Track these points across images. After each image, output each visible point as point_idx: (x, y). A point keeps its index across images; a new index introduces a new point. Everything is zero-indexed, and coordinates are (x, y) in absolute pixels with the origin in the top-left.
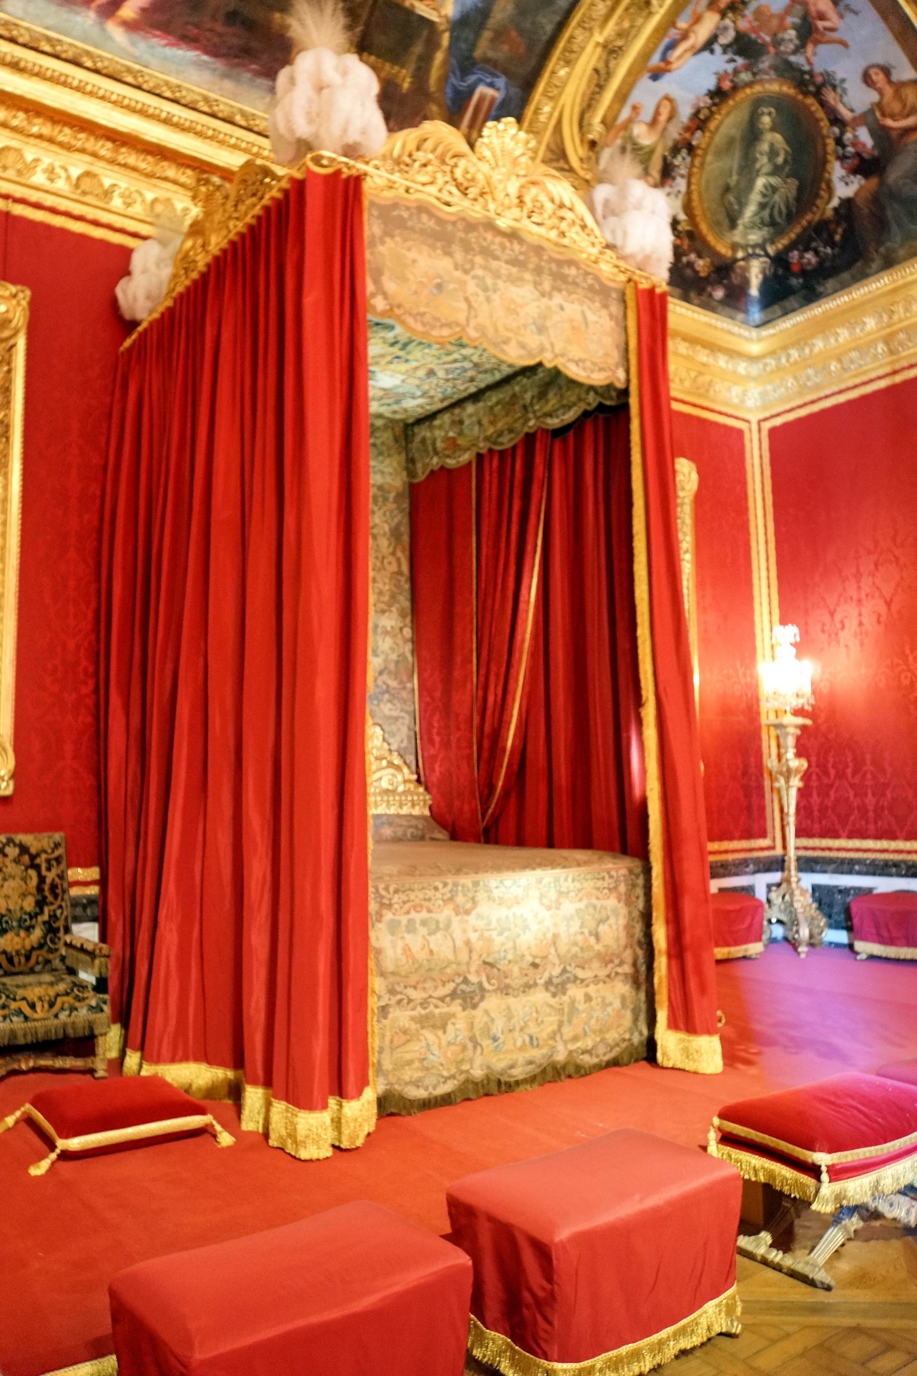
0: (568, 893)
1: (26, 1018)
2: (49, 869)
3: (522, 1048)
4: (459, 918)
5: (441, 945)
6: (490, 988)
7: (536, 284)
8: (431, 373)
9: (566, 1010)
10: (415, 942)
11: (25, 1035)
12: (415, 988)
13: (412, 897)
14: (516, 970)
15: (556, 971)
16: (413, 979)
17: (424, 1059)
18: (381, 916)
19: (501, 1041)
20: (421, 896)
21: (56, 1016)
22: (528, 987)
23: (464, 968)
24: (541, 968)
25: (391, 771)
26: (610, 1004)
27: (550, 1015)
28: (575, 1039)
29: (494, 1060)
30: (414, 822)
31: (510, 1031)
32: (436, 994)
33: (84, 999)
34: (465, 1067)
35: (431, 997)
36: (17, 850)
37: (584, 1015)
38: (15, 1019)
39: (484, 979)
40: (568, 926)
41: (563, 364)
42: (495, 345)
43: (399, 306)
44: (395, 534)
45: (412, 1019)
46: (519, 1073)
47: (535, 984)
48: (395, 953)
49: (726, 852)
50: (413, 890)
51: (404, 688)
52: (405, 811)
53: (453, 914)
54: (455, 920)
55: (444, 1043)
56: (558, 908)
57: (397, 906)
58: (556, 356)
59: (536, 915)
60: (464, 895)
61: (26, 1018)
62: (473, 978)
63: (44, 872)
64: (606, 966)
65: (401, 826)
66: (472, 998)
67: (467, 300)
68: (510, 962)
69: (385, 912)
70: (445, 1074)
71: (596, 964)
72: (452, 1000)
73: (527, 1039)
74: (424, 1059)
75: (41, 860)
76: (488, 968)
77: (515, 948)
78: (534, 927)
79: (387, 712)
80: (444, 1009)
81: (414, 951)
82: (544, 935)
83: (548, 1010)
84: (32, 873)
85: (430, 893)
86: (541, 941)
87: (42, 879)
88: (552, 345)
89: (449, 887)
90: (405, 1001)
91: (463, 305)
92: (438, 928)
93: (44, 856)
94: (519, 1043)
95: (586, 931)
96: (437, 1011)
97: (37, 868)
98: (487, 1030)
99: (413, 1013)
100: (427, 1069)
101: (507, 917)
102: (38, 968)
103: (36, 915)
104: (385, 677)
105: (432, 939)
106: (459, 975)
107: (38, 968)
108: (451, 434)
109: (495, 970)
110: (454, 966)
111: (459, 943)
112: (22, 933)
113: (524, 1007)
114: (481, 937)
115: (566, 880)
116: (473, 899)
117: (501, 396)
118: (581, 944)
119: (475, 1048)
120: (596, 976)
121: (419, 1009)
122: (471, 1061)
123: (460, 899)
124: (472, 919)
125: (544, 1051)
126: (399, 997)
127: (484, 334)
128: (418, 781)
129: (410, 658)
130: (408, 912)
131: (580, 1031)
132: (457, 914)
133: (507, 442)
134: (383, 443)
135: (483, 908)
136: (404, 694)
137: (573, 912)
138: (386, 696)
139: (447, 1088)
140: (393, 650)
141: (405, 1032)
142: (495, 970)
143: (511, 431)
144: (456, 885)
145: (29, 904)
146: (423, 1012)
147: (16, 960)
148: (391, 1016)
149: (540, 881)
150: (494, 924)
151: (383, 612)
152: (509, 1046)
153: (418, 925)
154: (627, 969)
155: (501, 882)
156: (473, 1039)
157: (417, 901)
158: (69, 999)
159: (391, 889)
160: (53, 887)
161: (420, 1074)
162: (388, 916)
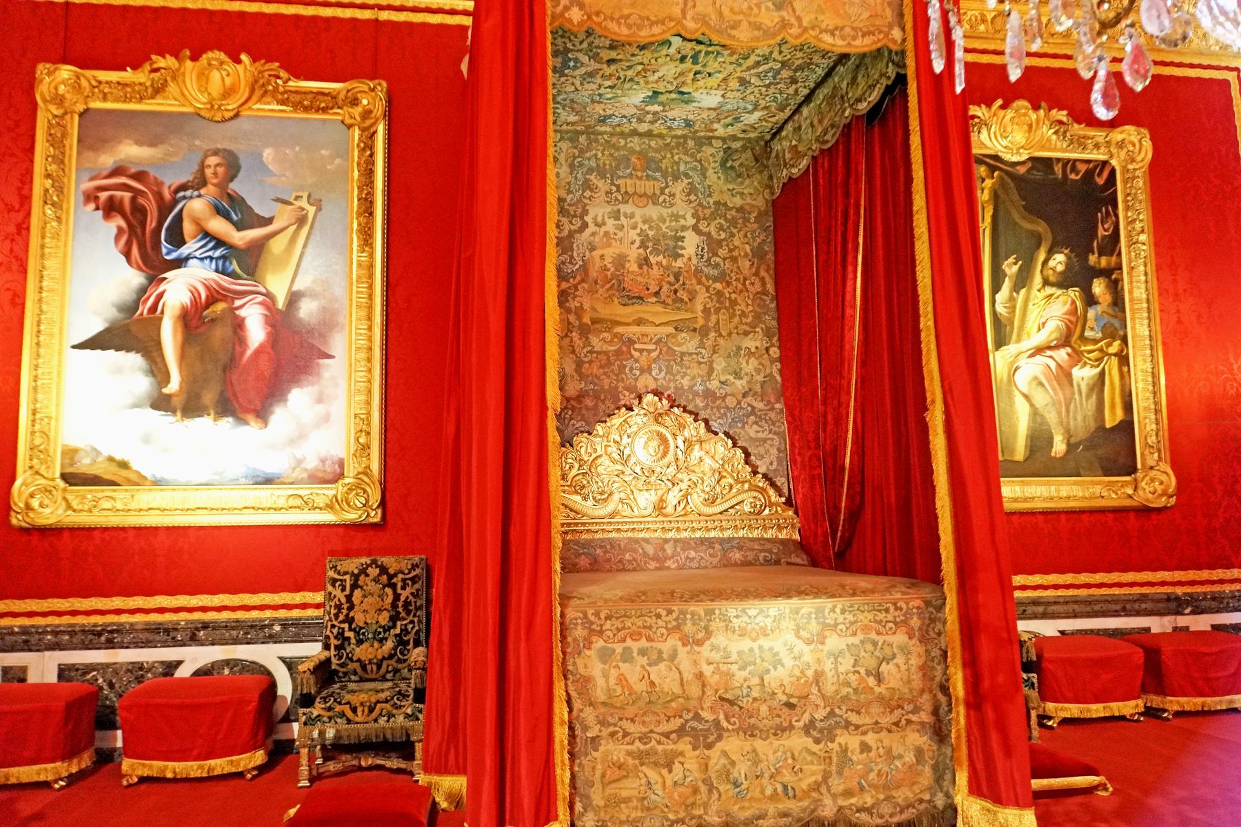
0: (836, 625)
1: (349, 721)
2: (403, 588)
3: (774, 797)
6: (730, 727)
8: (743, 82)
9: (835, 759)
11: (377, 737)
12: (633, 721)
13: (628, 624)
14: (764, 709)
15: (820, 714)
16: (631, 711)
17: (644, 799)
19: (743, 787)
20: (640, 624)
21: (376, 720)
22: (781, 730)
23: (694, 703)
24: (798, 710)
25: (755, 494)
26: (900, 757)
27: (812, 763)
28: (848, 793)
29: (736, 808)
30: (768, 546)
31: (757, 777)
32: (658, 730)
33: (401, 707)
34: (697, 812)
35: (652, 731)
36: (378, 570)
37: (860, 767)
38: (339, 720)
39: (722, 717)
40: (836, 662)
41: (816, 37)
42: (720, 32)
44: (758, 253)
45: (629, 753)
47: (791, 727)
48: (607, 682)
49: (1221, 582)
50: (629, 617)
51: (773, 409)
52: (770, 534)
53: (679, 643)
54: (682, 651)
55: (669, 783)
58: (805, 30)
59: (791, 650)
60: (694, 624)
61: (349, 721)
62: (706, 715)
63: (399, 591)
64: (891, 712)
65: (753, 550)
66: (706, 737)
68: (755, 699)
69: (594, 639)
70: (671, 816)
71: (876, 709)
72: (679, 737)
73: (780, 789)
74: (644, 799)
75: (398, 580)
76: (727, 705)
77: (762, 684)
78: (789, 663)
79: (753, 435)
81: (631, 681)
82: (802, 672)
83: (809, 758)
84: (388, 590)
85: (650, 621)
86: (799, 679)
87: (397, 597)
88: (799, 19)
89: (675, 615)
90: (620, 734)
92: (660, 659)
93: (400, 576)
94: (769, 791)
95: (862, 671)
96: (660, 748)
97: (393, 587)
98: (726, 774)
99: (629, 747)
100: (648, 809)
101: (751, 650)
102: (389, 676)
103: (390, 628)
104: (749, 399)
105: (653, 670)
106: (689, 711)
107: (389, 676)
108: (794, 143)
109: (737, 709)
111: (688, 676)
112: (376, 644)
113: (775, 752)
115: (833, 610)
116: (706, 628)
117: (826, 91)
118: (854, 685)
119: (710, 791)
120: (877, 723)
121: (637, 743)
122: (706, 806)
123: (689, 628)
124: (705, 650)
125: (805, 803)
126: (611, 729)
127: (706, 23)
128: (788, 503)
129: (778, 378)
130: (623, 640)
131: (854, 784)
132: (684, 645)
133: (831, 139)
134: (741, 165)
135: (719, 639)
136: (772, 415)
138: (752, 418)
140: (758, 371)
143: (833, 126)
144: (683, 613)
145: (384, 618)
146: (642, 747)
147: (369, 667)
148: (602, 749)
150: (734, 657)
151: (746, 334)
152: (757, 794)
153: (635, 654)
154: (925, 717)
155: (744, 611)
156: (707, 781)
157: (634, 628)
158: (388, 706)
159: (603, 615)
160: (407, 604)
161: (639, 814)
162: (599, 643)
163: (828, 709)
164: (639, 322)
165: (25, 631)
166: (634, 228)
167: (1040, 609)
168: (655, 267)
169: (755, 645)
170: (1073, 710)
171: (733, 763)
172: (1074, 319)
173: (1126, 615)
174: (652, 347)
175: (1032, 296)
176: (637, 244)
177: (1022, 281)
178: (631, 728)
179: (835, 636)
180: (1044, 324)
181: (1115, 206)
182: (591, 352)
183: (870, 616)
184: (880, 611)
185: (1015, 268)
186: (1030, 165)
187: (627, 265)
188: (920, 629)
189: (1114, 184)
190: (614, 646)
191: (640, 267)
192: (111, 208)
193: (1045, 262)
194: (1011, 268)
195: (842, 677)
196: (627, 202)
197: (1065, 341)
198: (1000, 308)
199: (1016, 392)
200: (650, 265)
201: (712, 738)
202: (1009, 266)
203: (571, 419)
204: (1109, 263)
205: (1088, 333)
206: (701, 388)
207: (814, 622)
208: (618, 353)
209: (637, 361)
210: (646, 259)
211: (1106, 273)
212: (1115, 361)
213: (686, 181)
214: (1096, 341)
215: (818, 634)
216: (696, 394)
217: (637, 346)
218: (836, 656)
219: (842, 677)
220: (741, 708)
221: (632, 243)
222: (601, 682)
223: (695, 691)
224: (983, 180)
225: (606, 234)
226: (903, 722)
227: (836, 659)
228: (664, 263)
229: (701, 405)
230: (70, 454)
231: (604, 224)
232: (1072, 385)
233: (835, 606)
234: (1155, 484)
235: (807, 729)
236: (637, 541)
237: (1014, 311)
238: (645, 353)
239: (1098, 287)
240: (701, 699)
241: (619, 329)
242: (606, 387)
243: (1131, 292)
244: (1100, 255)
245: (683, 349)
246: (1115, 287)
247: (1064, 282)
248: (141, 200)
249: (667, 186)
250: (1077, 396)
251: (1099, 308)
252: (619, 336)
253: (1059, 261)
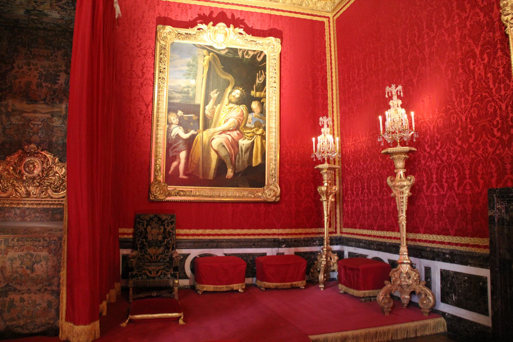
0: (13, 247)
26: (40, 304)
40: (12, 263)
56: (7, 254)
64: (37, 285)
95: (25, 267)
115: (13, 240)
120: (29, 289)
137: (17, 256)
163: (6, 283)
164: (35, 112)
166: (37, 70)
167: (215, 244)
168: (45, 88)
170: (210, 288)
172: (242, 118)
173: (255, 248)
174: (40, 123)
175: (223, 107)
176: (37, 77)
177: (219, 100)
179: (13, 251)
180: (227, 120)
181: (265, 71)
182: (10, 124)
183: (31, 243)
184: (36, 241)
185: (216, 95)
186: (227, 51)
187: (32, 86)
188: (55, 250)
189: (265, 61)
191: (37, 87)
193: (230, 93)
194: (214, 95)
195: (14, 269)
196: (34, 59)
197: (237, 128)
198: (207, 112)
199: (212, 149)
200: (42, 87)
202: (213, 94)
204: (260, 95)
205: (247, 125)
206: (61, 142)
208: (23, 125)
209: (32, 129)
210: (41, 84)
211: (259, 99)
212: (259, 138)
213: (63, 51)
214: (251, 129)
215: (5, 250)
216: (59, 144)
217: (32, 122)
218: (12, 260)
219: (14, 269)
221: (35, 76)
224: (205, 56)
225: (23, 72)
226: (43, 290)
227: (12, 261)
228: (49, 86)
229: (61, 149)
231: (22, 68)
232: (238, 148)
233: (14, 238)
234: (271, 191)
236: (13, 208)
237: (214, 114)
238: (36, 126)
239: (255, 105)
242: (17, 140)
243: (269, 108)
244: (256, 91)
245: (54, 124)
246: (262, 105)
247: (239, 102)
249: (54, 52)
250: (240, 152)
251: (254, 114)
252: (24, 118)
253: (237, 93)
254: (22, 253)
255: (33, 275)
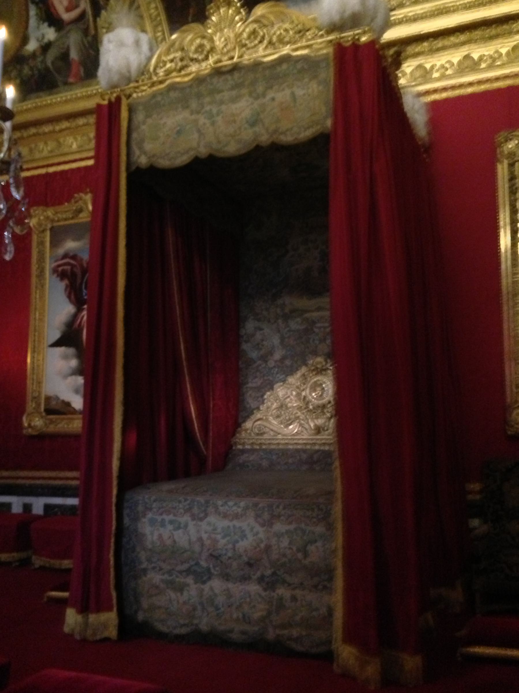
4: (194, 522)
5: (181, 538)
6: (216, 573)
7: (250, 94)
10: (166, 532)
12: (164, 561)
15: (269, 572)
18: (145, 515)
22: (245, 579)
26: (317, 609)
28: (283, 626)
31: (229, 606)
34: (196, 622)
39: (211, 566)
43: (154, 156)
45: (162, 581)
46: (235, 636)
53: (189, 519)
54: (191, 524)
56: (271, 527)
57: (155, 510)
59: (252, 529)
62: (203, 563)
67: (199, 131)
68: (230, 558)
80: (181, 579)
83: (260, 600)
89: (188, 502)
91: (196, 136)
92: (179, 528)
94: (235, 616)
95: (295, 549)
96: (177, 580)
105: (176, 533)
110: (189, 553)
114: (209, 538)
115: (278, 507)
123: (195, 510)
124: (204, 525)
126: (153, 565)
130: (161, 514)
135: (212, 519)
139: (183, 631)
141: (157, 587)
142: (219, 561)
148: (148, 576)
149: (256, 505)
153: (167, 523)
155: (226, 503)
156: (201, 604)
159: (152, 499)
162: (150, 515)
163: (273, 570)
165: (31, 486)
169: (231, 524)
171: (216, 595)
178: (164, 566)
190: (157, 517)
192: (62, 276)
201: (205, 578)
203: (277, 373)
207: (266, 514)
218: (279, 535)
220: (222, 562)
222: (149, 537)
223: (197, 548)
226: (320, 587)
230: (48, 399)
235: (261, 580)
240: (200, 553)
241: (307, 315)
248: (75, 270)
254: (292, 527)
255: (306, 562)
